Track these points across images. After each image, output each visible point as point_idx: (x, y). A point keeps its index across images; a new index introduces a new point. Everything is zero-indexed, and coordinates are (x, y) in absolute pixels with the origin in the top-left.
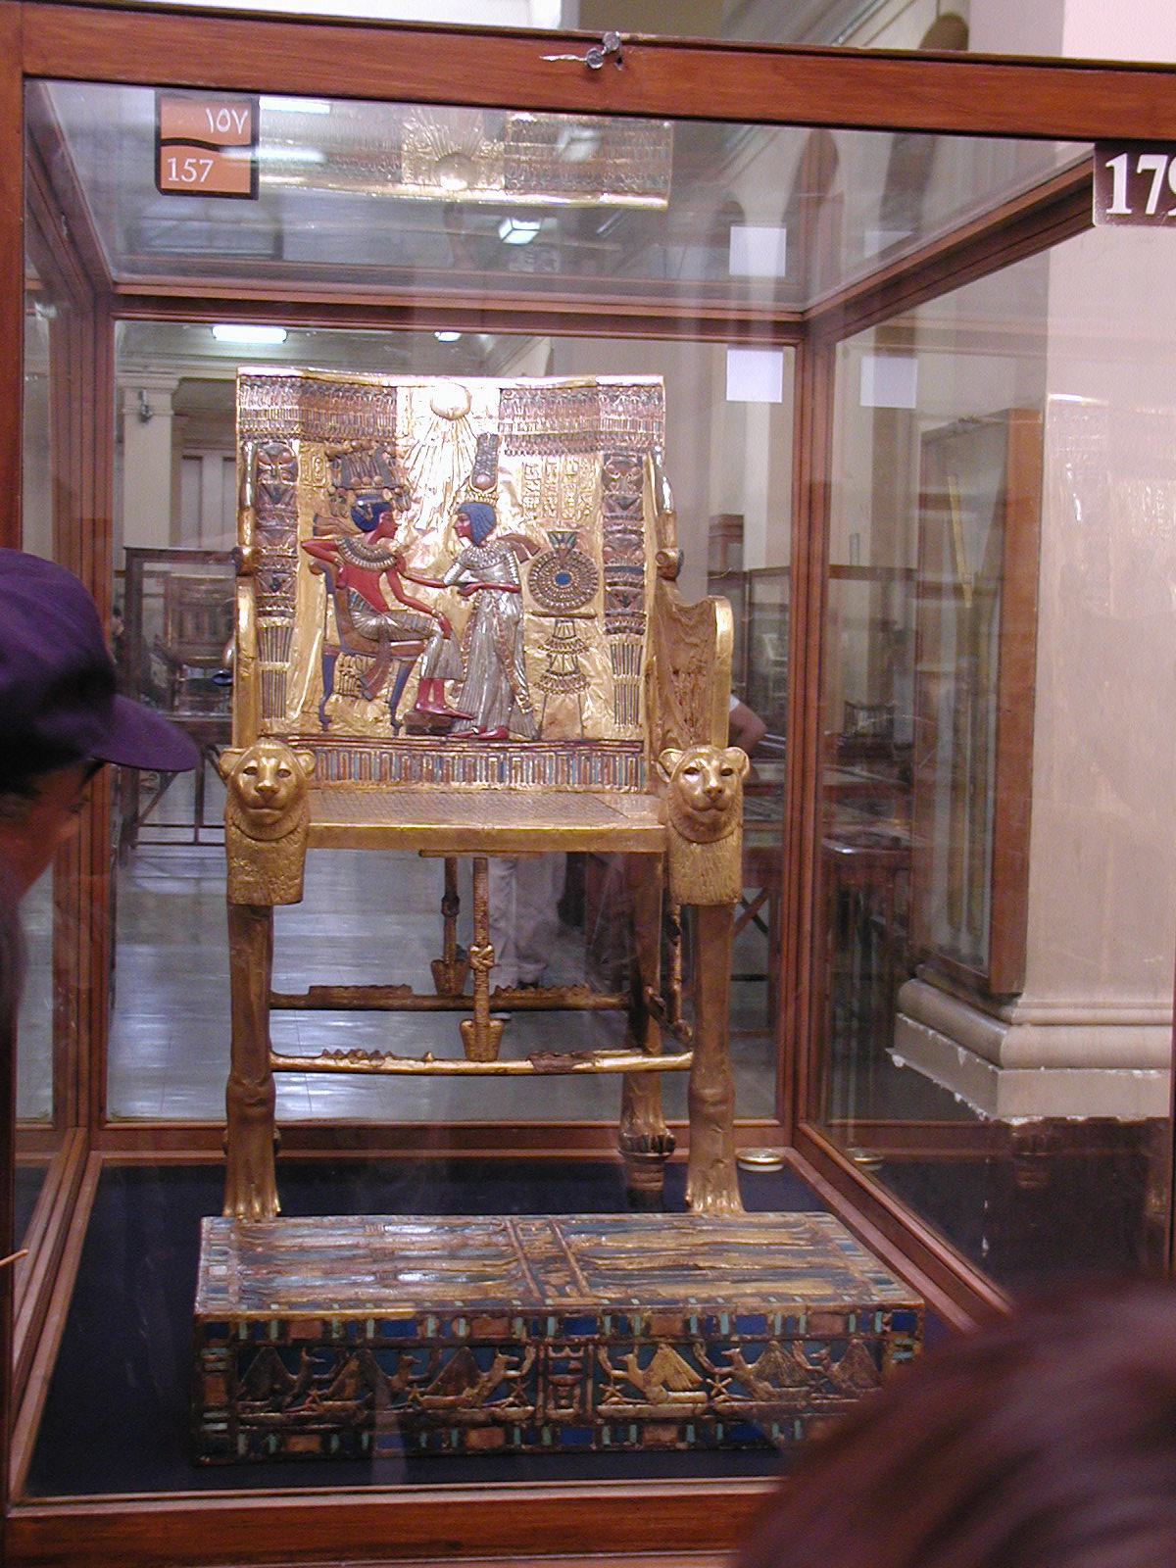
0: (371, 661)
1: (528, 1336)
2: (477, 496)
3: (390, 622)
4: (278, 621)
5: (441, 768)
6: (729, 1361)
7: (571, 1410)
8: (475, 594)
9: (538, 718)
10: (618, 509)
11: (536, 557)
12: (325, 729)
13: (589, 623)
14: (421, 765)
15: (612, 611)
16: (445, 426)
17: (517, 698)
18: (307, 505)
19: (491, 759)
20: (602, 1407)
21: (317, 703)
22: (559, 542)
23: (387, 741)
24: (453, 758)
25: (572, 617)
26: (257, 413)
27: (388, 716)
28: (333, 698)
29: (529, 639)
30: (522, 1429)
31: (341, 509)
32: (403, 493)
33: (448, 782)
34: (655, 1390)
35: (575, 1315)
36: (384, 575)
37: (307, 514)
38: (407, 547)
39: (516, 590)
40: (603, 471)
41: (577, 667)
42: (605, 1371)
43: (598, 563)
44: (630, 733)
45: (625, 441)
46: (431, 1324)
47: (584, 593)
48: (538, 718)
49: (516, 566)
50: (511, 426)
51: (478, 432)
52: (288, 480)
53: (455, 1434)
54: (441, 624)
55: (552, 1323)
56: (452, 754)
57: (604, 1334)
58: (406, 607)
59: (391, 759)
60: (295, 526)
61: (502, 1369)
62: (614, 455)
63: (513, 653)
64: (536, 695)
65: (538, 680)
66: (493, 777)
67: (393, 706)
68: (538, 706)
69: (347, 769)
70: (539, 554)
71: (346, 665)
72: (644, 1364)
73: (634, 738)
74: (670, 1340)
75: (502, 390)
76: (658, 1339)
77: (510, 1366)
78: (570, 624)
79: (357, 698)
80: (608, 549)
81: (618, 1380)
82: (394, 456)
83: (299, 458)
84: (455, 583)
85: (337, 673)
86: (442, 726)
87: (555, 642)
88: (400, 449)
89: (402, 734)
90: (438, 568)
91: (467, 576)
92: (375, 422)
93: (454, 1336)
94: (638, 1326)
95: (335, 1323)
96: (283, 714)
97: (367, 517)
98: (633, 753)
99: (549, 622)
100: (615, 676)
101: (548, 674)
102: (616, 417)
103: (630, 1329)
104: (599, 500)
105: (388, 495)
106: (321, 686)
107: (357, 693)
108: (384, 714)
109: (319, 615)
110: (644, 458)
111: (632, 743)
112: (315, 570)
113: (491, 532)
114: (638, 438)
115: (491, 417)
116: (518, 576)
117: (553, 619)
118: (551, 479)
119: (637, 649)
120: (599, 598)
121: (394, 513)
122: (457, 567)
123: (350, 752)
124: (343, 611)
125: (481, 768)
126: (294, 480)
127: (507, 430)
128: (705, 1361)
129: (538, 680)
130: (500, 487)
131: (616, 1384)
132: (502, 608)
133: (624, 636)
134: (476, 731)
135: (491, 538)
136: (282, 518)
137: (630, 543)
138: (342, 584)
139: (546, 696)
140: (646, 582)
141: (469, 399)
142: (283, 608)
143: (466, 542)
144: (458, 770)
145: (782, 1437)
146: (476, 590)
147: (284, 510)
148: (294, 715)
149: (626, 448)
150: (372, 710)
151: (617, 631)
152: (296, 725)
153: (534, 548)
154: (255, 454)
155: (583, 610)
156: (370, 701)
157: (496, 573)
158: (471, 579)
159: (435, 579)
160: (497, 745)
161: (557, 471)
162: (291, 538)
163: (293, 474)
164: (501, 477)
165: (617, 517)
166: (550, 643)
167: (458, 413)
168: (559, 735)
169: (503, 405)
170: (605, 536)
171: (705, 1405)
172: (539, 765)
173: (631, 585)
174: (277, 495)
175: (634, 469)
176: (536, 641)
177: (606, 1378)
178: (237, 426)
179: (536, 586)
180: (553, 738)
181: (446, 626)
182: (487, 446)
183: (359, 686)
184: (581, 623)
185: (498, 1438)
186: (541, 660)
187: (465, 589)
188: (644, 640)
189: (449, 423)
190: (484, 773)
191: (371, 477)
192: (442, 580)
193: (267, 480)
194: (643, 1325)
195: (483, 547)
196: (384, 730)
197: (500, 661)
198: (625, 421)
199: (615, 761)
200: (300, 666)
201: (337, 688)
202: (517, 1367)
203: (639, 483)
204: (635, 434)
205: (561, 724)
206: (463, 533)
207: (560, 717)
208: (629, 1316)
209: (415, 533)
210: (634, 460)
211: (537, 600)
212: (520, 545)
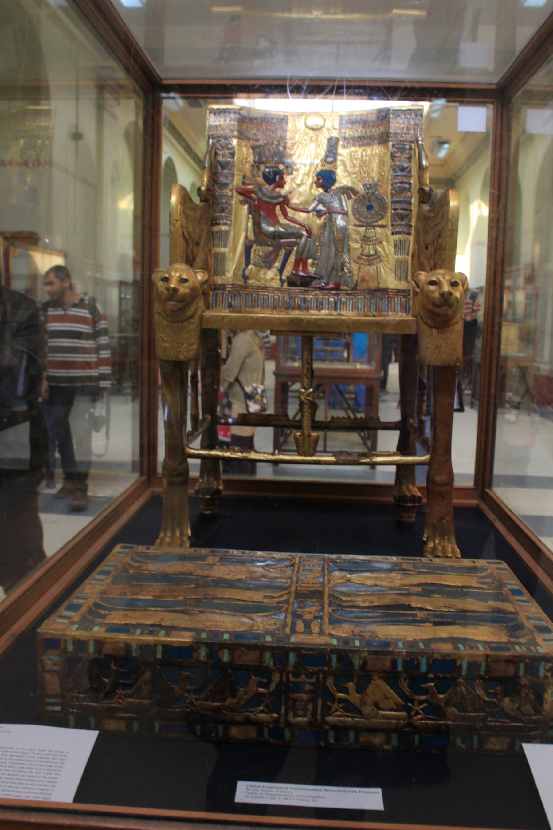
0: (270, 249)
1: (275, 664)
2: (327, 167)
3: (281, 230)
4: (223, 228)
5: (305, 303)
6: (426, 691)
7: (305, 719)
8: (324, 216)
9: (355, 278)
10: (398, 171)
11: (357, 197)
12: (245, 282)
13: (383, 230)
14: (295, 302)
15: (395, 223)
16: (311, 133)
18: (240, 170)
20: (329, 719)
21: (242, 269)
22: (368, 189)
23: (277, 289)
24: (311, 299)
25: (374, 227)
26: (216, 126)
27: (278, 277)
28: (250, 267)
30: (269, 728)
31: (258, 173)
32: (290, 168)
33: (308, 310)
34: (367, 710)
35: (311, 652)
37: (240, 175)
38: (290, 192)
39: (345, 214)
40: (392, 153)
42: (331, 693)
43: (388, 200)
44: (403, 285)
46: (203, 653)
47: (381, 214)
48: (355, 278)
49: (346, 202)
50: (345, 133)
51: (328, 137)
52: (230, 158)
53: (221, 728)
54: (307, 231)
55: (292, 657)
56: (311, 297)
57: (331, 667)
60: (233, 180)
61: (254, 686)
62: (398, 144)
63: (343, 246)
64: (355, 267)
65: (356, 259)
67: (281, 271)
68: (355, 272)
70: (358, 195)
72: (361, 690)
73: (405, 288)
74: (381, 675)
76: (372, 673)
77: (260, 685)
78: (373, 230)
79: (262, 267)
80: (393, 192)
81: (340, 700)
82: (285, 148)
83: (236, 148)
84: (314, 210)
85: (252, 254)
86: (305, 282)
87: (365, 239)
88: (289, 145)
89: (285, 286)
90: (307, 203)
91: (320, 207)
93: (220, 660)
94: (357, 662)
95: (134, 646)
96: (224, 274)
99: (362, 230)
100: (396, 257)
102: (398, 125)
103: (351, 664)
105: (281, 167)
106: (243, 260)
107: (262, 265)
109: (243, 226)
110: (413, 146)
111: (404, 291)
112: (242, 203)
113: (333, 184)
114: (410, 135)
115: (335, 129)
116: (347, 207)
117: (364, 228)
118: (364, 158)
119: (407, 243)
120: (389, 215)
121: (285, 176)
122: (316, 202)
123: (258, 295)
124: (257, 225)
126: (233, 157)
127: (343, 135)
128: (406, 690)
129: (356, 259)
130: (338, 163)
131: (339, 703)
132: (338, 222)
133: (400, 236)
134: (323, 285)
135: (333, 188)
136: (226, 177)
137: (405, 189)
138: (256, 210)
140: (413, 208)
141: (325, 120)
143: (321, 190)
144: (314, 305)
145: (463, 746)
146: (325, 214)
147: (228, 173)
148: (230, 274)
149: (404, 141)
150: (271, 274)
151: (397, 233)
152: (230, 280)
154: (213, 144)
155: (380, 223)
157: (336, 205)
158: (323, 209)
159: (305, 209)
160: (334, 292)
161: (368, 154)
162: (231, 187)
163: (233, 155)
164: (339, 158)
165: (398, 176)
166: (363, 240)
167: (318, 127)
169: (341, 124)
170: (392, 185)
171: (406, 721)
172: (355, 303)
173: (405, 210)
174: (224, 165)
175: (407, 151)
176: (356, 239)
177: (333, 699)
178: (207, 133)
179: (356, 212)
180: (363, 288)
181: (309, 232)
182: (332, 145)
183: (264, 262)
184: (379, 230)
185: (252, 733)
186: (358, 249)
187: (319, 214)
189: (313, 132)
190: (327, 306)
191: (273, 158)
192: (308, 209)
193: (220, 159)
194: (361, 662)
196: (276, 284)
197: (337, 249)
198: (403, 128)
199: (394, 300)
200: (234, 251)
201: (252, 262)
202: (266, 686)
203: (410, 158)
204: (408, 134)
206: (319, 185)
207: (367, 278)
208: (350, 655)
209: (295, 186)
210: (408, 147)
211: (356, 219)
212: (347, 191)
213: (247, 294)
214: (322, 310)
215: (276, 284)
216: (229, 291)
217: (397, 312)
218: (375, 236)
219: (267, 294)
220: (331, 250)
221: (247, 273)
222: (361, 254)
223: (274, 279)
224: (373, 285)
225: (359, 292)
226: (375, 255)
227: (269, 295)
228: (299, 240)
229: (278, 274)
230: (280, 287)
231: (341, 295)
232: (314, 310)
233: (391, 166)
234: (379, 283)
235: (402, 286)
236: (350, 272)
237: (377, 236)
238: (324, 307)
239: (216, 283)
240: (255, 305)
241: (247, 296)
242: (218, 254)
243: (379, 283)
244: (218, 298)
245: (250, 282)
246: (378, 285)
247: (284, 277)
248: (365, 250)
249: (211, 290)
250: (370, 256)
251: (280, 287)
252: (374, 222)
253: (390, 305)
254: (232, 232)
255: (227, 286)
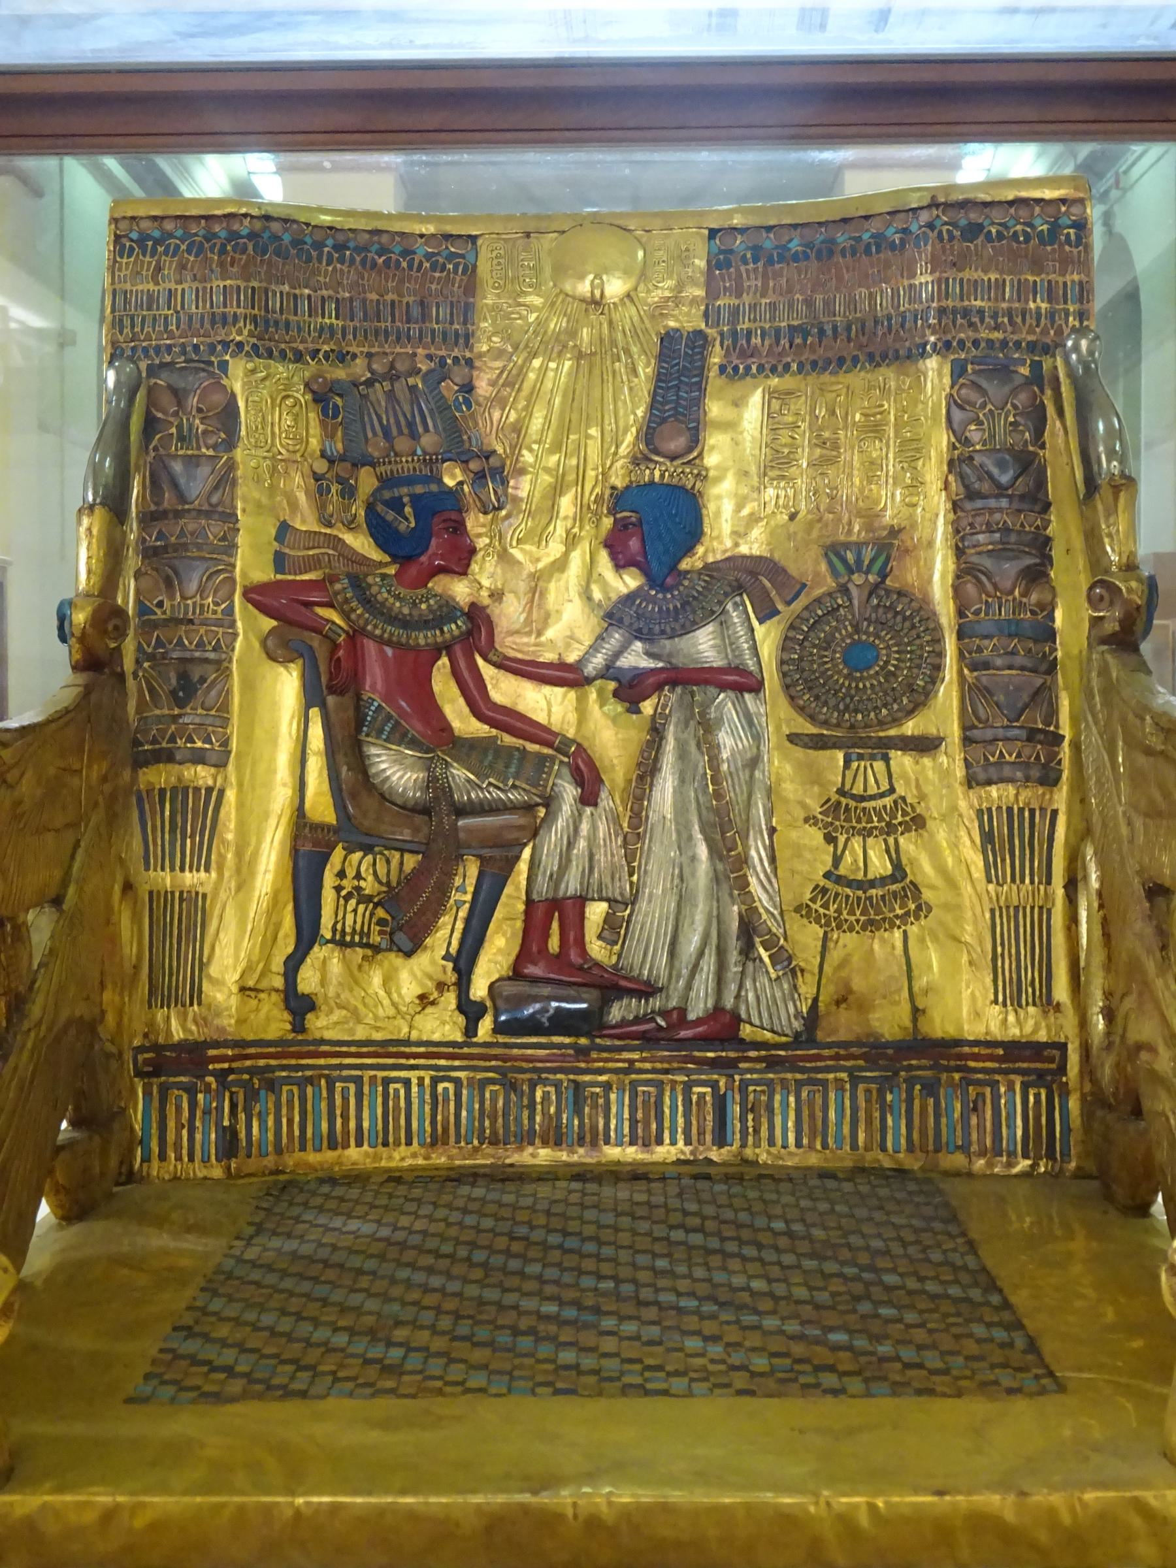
0: (411, 861)
5: (578, 1111)
9: (807, 989)
11: (798, 605)
12: (299, 1026)
17: (757, 940)
19: (696, 1090)
21: (278, 964)
24: (607, 1087)
25: (883, 748)
33: (594, 1144)
36: (444, 661)
41: (898, 866)
45: (997, 328)
56: (604, 1078)
58: (494, 732)
59: (458, 1095)
64: (806, 938)
66: (702, 1133)
69: (352, 1125)
71: (351, 873)
73: (1042, 1036)
75: (713, 233)
78: (879, 765)
79: (377, 949)
84: (608, 671)
92: (425, 317)
96: (196, 995)
97: (403, 527)
98: (1041, 1075)
100: (991, 887)
101: (829, 885)
104: (945, 468)
107: (376, 939)
108: (441, 986)
111: (1034, 1050)
113: (689, 550)
125: (674, 1108)
133: (1011, 790)
139: (826, 933)
140: (1059, 654)
142: (199, 744)
149: (1004, 343)
153: (793, 587)
155: (910, 728)
156: (409, 954)
160: (711, 1055)
168: (857, 1029)
170: (959, 552)
180: (843, 1035)
184: (902, 761)
188: (1061, 798)
191: (414, 436)
195: (669, 589)
196: (441, 1024)
200: (244, 882)
205: (864, 1007)
210: (1025, 371)
211: (801, 710)
213: (310, 1080)
214: (660, 1142)
215: (441, 1024)
216: (221, 1075)
217: (1012, 1154)
218: (892, 790)
219: (403, 1074)
220: (694, 858)
221: (308, 980)
222: (827, 875)
223: (433, 1003)
224: (890, 1021)
225: (826, 1052)
226: (893, 879)
227: (413, 1075)
228: (542, 812)
229: (452, 977)
230: (459, 1037)
231: (741, 1065)
232: (619, 1144)
233: (951, 463)
234: (917, 1012)
235: (1029, 1027)
236: (783, 958)
237: (900, 790)
238: (667, 1124)
239: (161, 1040)
240: (346, 1132)
241: (309, 1089)
242: (168, 896)
243: (917, 1012)
244: (171, 1110)
245: (322, 1025)
246: (915, 1020)
247: (479, 990)
248: (848, 858)
249: (139, 1074)
250: (872, 884)
251: (459, 1037)
252: (882, 724)
253: (974, 1120)
254: (231, 795)
255: (212, 1052)
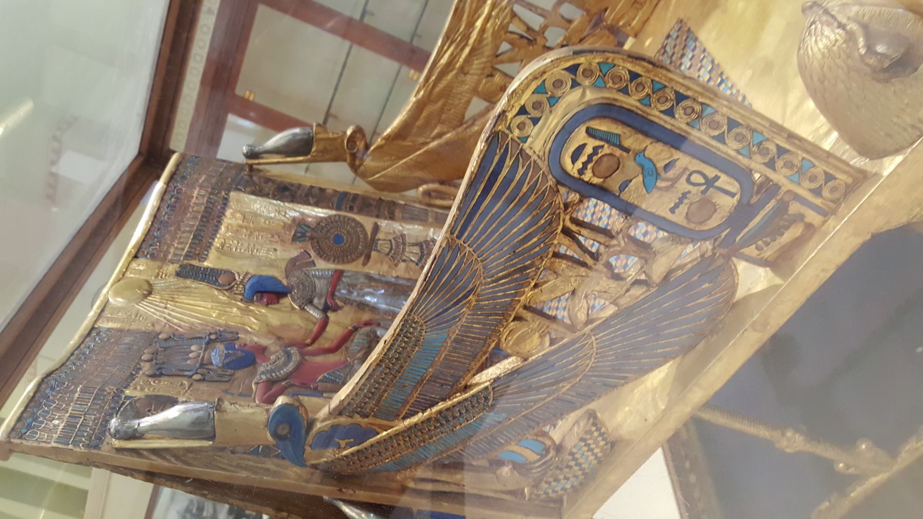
29: (387, 272)
78: (380, 242)
135: (285, 282)
184: (380, 236)
211: (353, 260)
250: (422, 253)
